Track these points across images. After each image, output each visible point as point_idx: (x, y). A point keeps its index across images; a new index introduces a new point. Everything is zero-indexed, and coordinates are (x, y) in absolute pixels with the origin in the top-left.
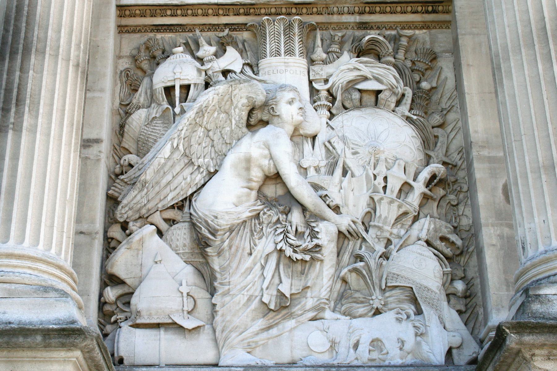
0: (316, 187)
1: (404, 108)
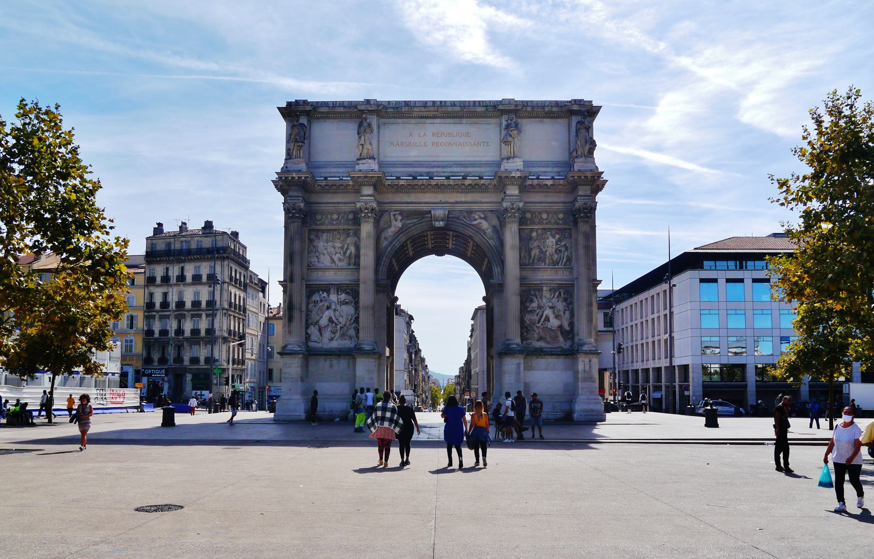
0: (337, 319)
1: (352, 304)
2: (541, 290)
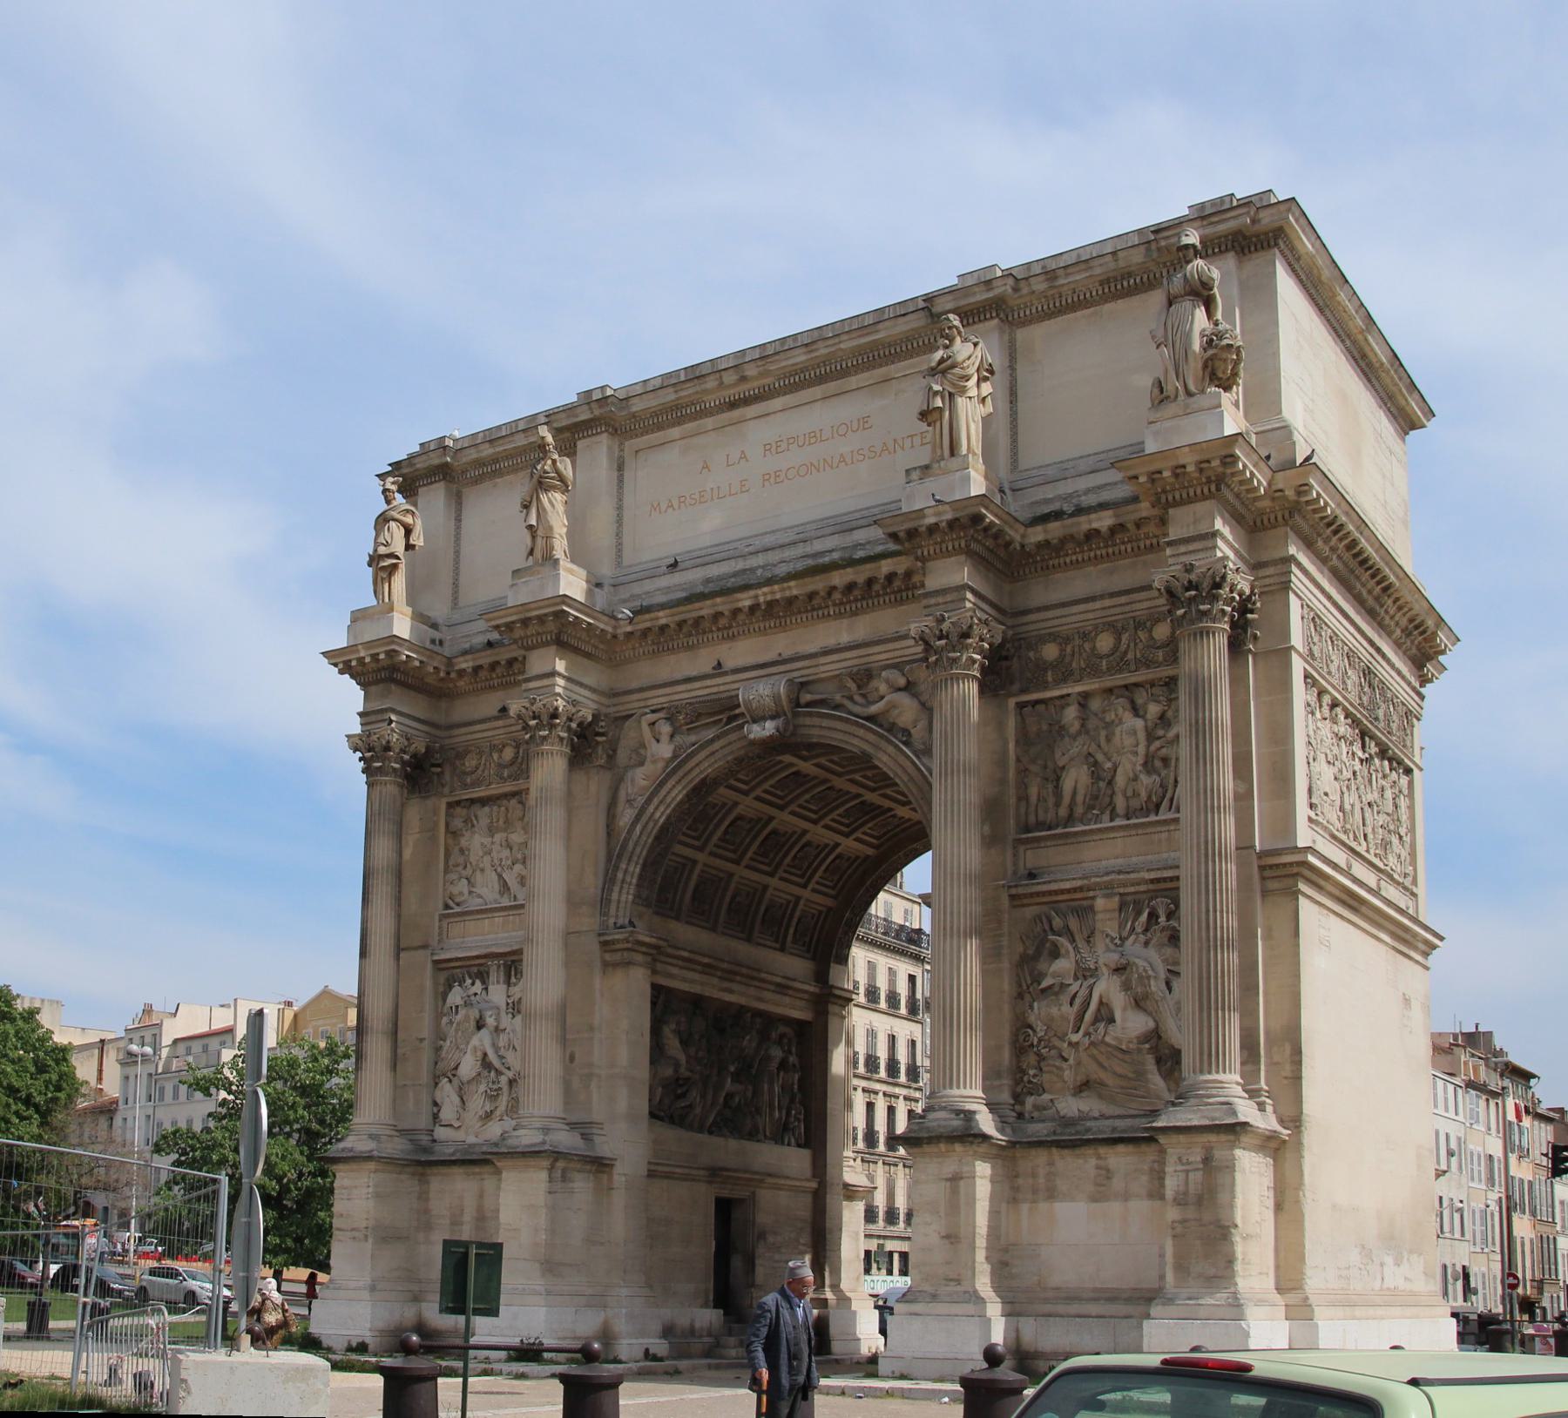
0: (502, 1057)
2: (1085, 911)
